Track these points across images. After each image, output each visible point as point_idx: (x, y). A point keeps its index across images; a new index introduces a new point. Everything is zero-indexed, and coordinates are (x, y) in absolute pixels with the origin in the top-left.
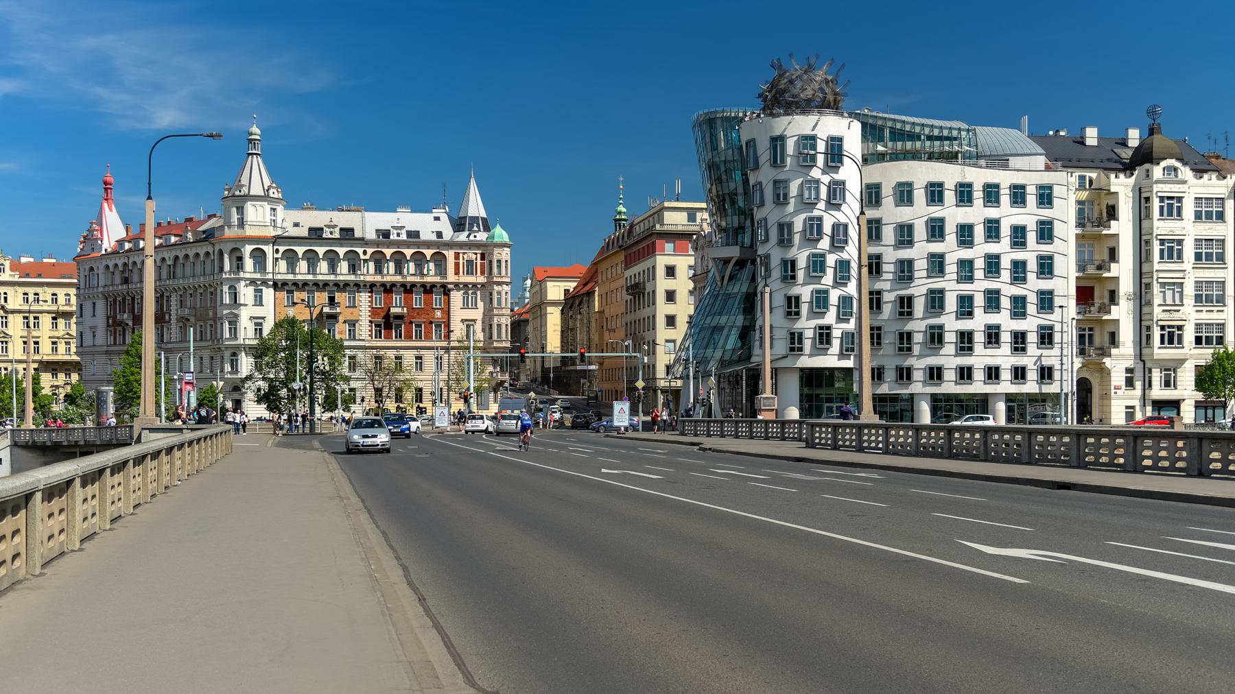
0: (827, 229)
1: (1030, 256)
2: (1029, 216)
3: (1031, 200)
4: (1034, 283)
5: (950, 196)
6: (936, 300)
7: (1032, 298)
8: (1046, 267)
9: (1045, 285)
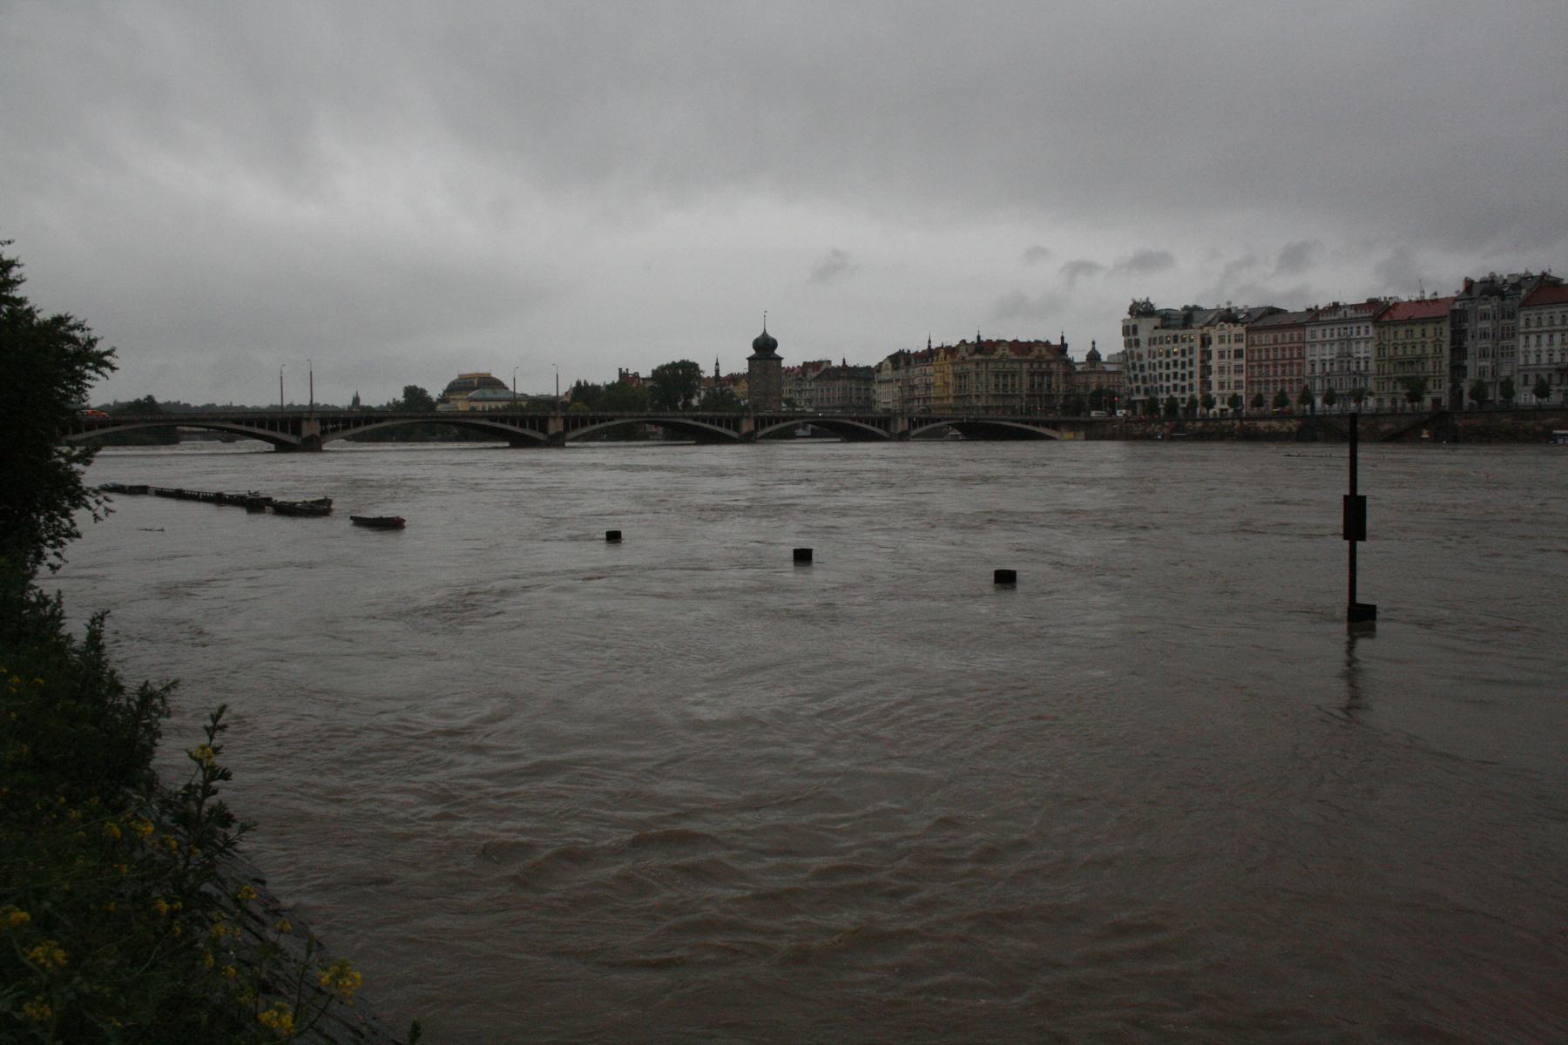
0: (1135, 355)
1: (1186, 360)
2: (1185, 346)
4: (1188, 369)
6: (1161, 375)
7: (1187, 374)
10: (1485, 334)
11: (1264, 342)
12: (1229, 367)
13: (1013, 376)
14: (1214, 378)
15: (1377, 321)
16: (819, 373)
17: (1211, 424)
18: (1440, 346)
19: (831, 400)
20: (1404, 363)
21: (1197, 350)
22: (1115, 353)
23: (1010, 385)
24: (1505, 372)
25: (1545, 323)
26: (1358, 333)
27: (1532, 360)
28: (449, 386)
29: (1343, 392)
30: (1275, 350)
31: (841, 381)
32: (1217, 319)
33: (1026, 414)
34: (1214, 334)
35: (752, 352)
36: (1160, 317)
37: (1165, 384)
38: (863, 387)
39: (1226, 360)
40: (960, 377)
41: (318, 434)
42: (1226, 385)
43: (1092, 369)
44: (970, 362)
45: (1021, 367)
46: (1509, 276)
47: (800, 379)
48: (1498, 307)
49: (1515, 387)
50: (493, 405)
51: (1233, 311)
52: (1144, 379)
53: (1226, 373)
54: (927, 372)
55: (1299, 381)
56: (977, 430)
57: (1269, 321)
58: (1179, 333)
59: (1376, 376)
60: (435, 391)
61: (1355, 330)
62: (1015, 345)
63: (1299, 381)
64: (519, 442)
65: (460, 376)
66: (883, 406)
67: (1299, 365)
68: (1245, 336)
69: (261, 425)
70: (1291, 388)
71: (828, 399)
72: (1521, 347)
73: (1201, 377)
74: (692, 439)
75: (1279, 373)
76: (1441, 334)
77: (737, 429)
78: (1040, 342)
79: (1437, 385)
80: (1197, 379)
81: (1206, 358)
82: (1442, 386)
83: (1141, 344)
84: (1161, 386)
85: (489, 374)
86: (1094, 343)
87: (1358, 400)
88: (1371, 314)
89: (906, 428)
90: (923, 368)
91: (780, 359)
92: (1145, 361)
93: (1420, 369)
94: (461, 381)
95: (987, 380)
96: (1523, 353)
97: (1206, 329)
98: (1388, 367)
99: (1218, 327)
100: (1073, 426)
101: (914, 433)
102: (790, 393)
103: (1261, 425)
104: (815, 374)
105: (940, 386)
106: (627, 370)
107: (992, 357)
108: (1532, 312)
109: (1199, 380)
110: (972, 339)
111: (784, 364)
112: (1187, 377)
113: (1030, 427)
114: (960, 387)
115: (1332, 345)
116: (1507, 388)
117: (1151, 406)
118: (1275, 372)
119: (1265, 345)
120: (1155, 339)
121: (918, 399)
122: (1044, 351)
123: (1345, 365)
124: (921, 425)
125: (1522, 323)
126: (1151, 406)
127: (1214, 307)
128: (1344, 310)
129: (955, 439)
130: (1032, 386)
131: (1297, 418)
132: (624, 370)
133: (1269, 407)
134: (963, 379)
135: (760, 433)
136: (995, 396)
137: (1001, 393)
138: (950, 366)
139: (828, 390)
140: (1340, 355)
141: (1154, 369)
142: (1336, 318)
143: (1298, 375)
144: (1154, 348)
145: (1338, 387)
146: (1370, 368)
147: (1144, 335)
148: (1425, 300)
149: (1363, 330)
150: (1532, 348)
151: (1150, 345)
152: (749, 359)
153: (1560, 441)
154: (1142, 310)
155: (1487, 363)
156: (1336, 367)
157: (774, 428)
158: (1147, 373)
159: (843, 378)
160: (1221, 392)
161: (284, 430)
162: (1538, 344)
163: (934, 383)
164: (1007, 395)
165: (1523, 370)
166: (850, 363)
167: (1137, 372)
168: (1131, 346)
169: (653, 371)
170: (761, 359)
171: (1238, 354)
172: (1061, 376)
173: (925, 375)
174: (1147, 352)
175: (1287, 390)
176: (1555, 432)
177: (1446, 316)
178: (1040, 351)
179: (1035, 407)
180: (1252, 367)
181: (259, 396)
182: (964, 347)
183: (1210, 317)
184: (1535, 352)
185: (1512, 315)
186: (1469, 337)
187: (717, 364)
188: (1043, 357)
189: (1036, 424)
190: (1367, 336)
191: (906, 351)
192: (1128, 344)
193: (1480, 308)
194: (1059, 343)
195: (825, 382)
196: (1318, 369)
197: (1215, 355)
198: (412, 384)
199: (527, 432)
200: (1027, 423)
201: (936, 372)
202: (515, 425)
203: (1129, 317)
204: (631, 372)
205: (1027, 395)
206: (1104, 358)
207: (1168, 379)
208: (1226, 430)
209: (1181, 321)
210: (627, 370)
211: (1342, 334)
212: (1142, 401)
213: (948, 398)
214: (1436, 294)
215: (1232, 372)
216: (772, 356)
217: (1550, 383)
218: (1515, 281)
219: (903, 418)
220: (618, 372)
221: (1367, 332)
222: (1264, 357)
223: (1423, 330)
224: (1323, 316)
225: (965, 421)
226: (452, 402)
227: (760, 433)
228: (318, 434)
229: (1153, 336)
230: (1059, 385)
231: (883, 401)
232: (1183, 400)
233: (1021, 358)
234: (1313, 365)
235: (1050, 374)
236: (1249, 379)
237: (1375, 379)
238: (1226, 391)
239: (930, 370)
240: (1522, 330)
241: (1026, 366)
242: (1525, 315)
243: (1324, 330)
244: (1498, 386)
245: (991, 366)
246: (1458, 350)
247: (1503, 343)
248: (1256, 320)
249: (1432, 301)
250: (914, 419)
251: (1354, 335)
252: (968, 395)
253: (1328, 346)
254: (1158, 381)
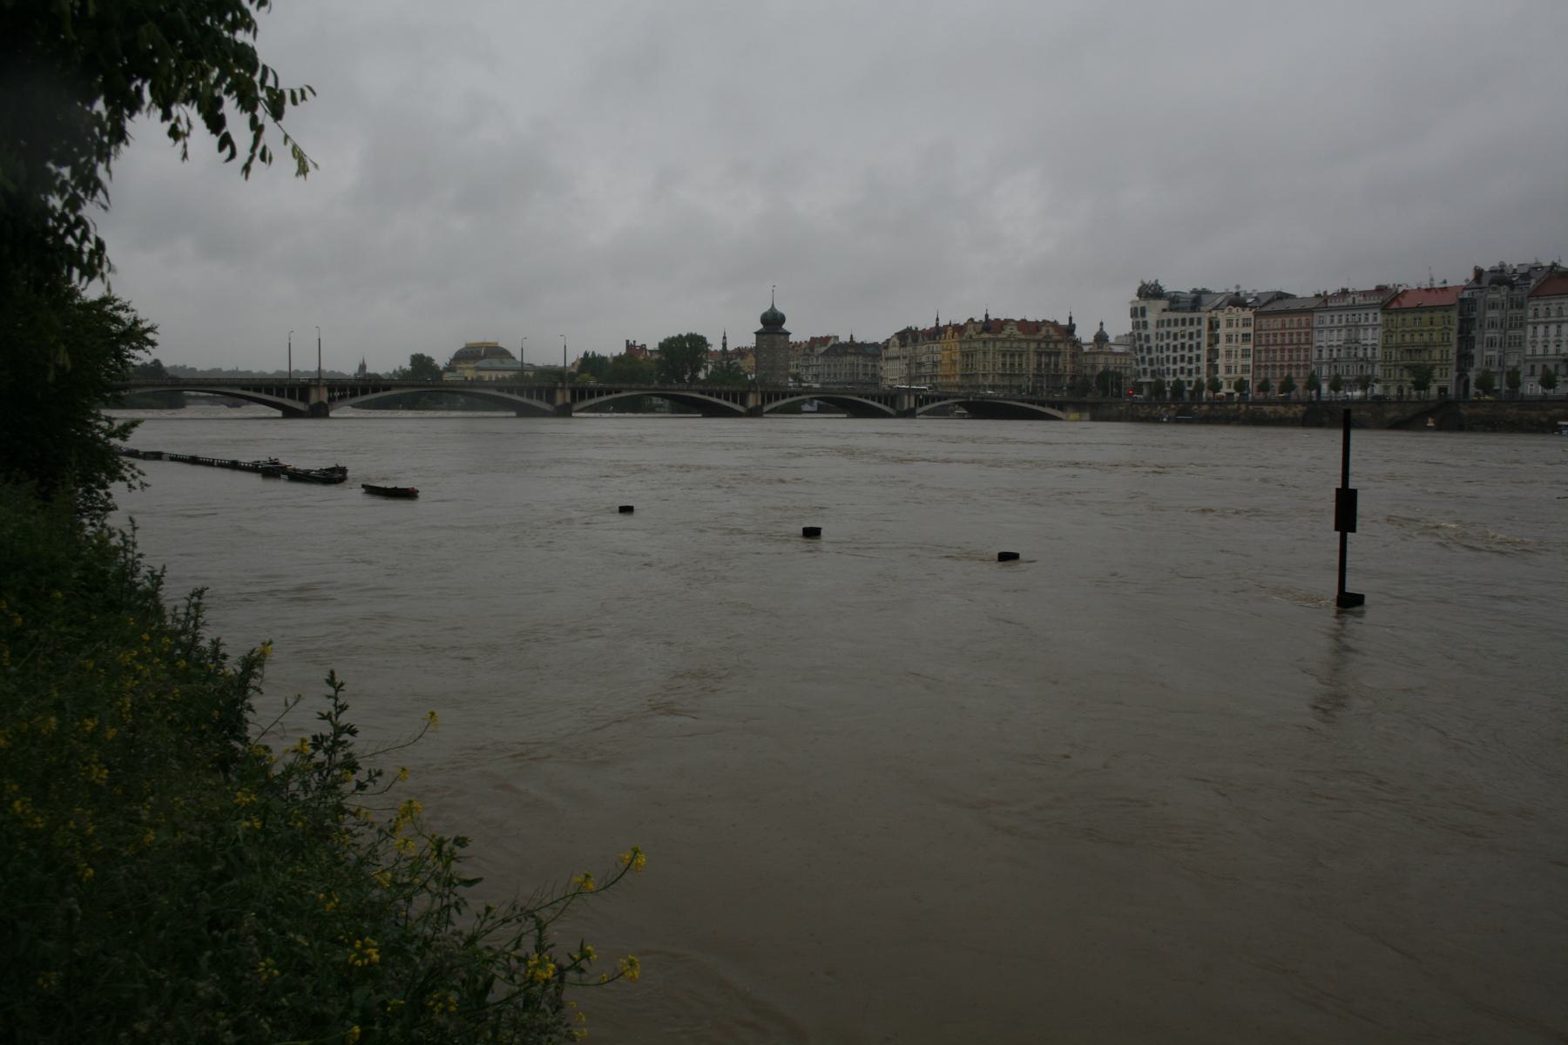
0: (1143, 336)
1: (1194, 343)
2: (1193, 329)
3: (1195, 323)
4: (1195, 352)
5: (1172, 323)
6: (1168, 357)
7: (1194, 357)
8: (1199, 345)
9: (1199, 352)
10: (1493, 323)
11: (1271, 327)
12: (1236, 351)
13: (1020, 356)
14: (1221, 362)
15: (1385, 308)
16: (825, 348)
17: (1217, 407)
18: (1448, 334)
19: (838, 376)
20: (1411, 350)
21: (1205, 333)
22: (1123, 334)
23: (1017, 364)
24: (1512, 362)
25: (1553, 314)
26: (1367, 319)
27: (1540, 350)
28: (456, 354)
29: (1350, 378)
30: (1283, 335)
31: (848, 358)
32: (1226, 303)
33: (1031, 394)
34: (1222, 317)
35: (760, 327)
36: (1168, 299)
37: (1172, 367)
39: (1233, 344)
40: (967, 355)
41: (326, 401)
42: (1233, 369)
43: (1100, 350)
44: (977, 340)
45: (1028, 347)
46: (1519, 265)
47: (807, 354)
48: (1507, 296)
49: (1521, 376)
50: (500, 374)
51: (1242, 295)
52: (1151, 360)
53: (1233, 356)
54: (935, 349)
55: (1306, 367)
56: (981, 409)
57: (1277, 306)
58: (1188, 316)
59: (1382, 363)
60: (441, 360)
61: (1363, 317)
62: (1023, 325)
63: (1306, 367)
64: (525, 412)
65: (466, 345)
66: (890, 383)
67: (1306, 350)
68: (1253, 319)
69: (269, 392)
70: (1298, 373)
71: (835, 375)
72: (1529, 338)
73: (1209, 360)
74: (699, 413)
75: (1286, 358)
76: (1449, 322)
77: (743, 403)
78: (1048, 322)
79: (1444, 374)
80: (1204, 363)
81: (1213, 342)
82: (1449, 374)
83: (1149, 326)
84: (1168, 369)
85: (497, 343)
86: (1102, 324)
87: (1364, 388)
88: (1380, 301)
89: (912, 405)
90: (931, 345)
91: (788, 334)
92: (1153, 343)
93: (1427, 357)
94: (468, 350)
95: (994, 358)
96: (1531, 342)
97: (1214, 312)
98: (1396, 355)
99: (1226, 311)
100: (1079, 407)
101: (919, 410)
102: (797, 367)
103: (1267, 409)
104: (823, 349)
105: (946, 364)
106: (634, 342)
107: (1000, 336)
108: (1542, 303)
109: (1206, 363)
110: (979, 317)
111: (792, 339)
112: (1194, 361)
113: (1035, 407)
114: (967, 365)
115: (1339, 331)
116: (1514, 379)
117: (1158, 388)
118: (1282, 357)
119: (1274, 329)
120: (1163, 321)
121: (925, 377)
122: (1052, 331)
123: (1353, 352)
124: (927, 403)
125: (1531, 313)
126: (1158, 388)
127: (1223, 291)
128: (1352, 296)
129: (961, 416)
130: (1039, 365)
131: (1304, 404)
132: (631, 342)
133: (1275, 393)
134: (970, 357)
135: (766, 408)
137: (1008, 372)
138: (957, 343)
139: (835, 365)
140: (1348, 341)
141: (1162, 352)
142: (1345, 304)
143: (1305, 361)
144: (1162, 330)
145: (1345, 373)
146: (1377, 355)
147: (1152, 317)
148: (1434, 289)
149: (1371, 317)
150: (1540, 338)
151: (1157, 327)
152: (756, 333)
153: (1565, 432)
154: (1150, 292)
155: (1494, 353)
156: (1343, 354)
157: (782, 402)
158: (1154, 355)
159: (851, 354)
160: (1229, 376)
161: (291, 396)
162: (1546, 334)
163: (940, 361)
164: (1015, 375)
165: (1531, 361)
166: (858, 340)
167: (1145, 353)
168: (1139, 328)
169: (660, 344)
170: (769, 333)
171: (1246, 337)
172: (1068, 358)
173: (932, 352)
174: (1155, 335)
175: (1294, 375)
176: (1560, 423)
177: (1453, 305)
178: (1048, 331)
179: (1042, 387)
180: (1260, 352)
181: (267, 362)
182: (972, 326)
183: (1218, 301)
184: (1543, 342)
185: (1521, 306)
186: (1477, 324)
187: (725, 338)
188: (1050, 337)
189: (1042, 404)
190: (1375, 323)
191: (914, 328)
192: (1136, 326)
193: (1490, 296)
194: (1067, 323)
195: (832, 358)
196: (1325, 354)
197: (1223, 339)
198: (419, 353)
199: (535, 402)
200: (1033, 403)
201: (943, 350)
202: (521, 395)
203: (1137, 298)
204: (638, 344)
205: (1034, 375)
206: (1112, 339)
207: (1175, 361)
208: (1232, 414)
209: (1188, 305)
210: (634, 342)
211: (1350, 320)
212: (1150, 383)
213: (954, 376)
214: (1445, 282)
215: (1239, 357)
216: (780, 331)
217: (1557, 374)
218: (1525, 270)
219: (909, 396)
220: (625, 343)
221: (1375, 319)
222: (1271, 342)
223: (1432, 318)
224: (1331, 302)
225: (971, 399)
226: (458, 371)
227: (766, 408)
228: (326, 401)
229: (1161, 319)
230: (1066, 365)
231: (890, 377)
232: (1190, 383)
233: (1031, 337)
234: (1320, 351)
235: (1058, 354)
236: (1257, 364)
237: (1382, 366)
238: (1233, 375)
239: (937, 347)
240: (1530, 320)
241: (1033, 346)
242: (1533, 305)
243: (1332, 316)
244: (1504, 377)
245: (998, 345)
246: (1466, 338)
247: (1511, 332)
248: (1266, 304)
249: (1440, 289)
250: (921, 397)
251: (1362, 322)
252: (977, 374)
253: (1335, 332)
254: (1165, 363)
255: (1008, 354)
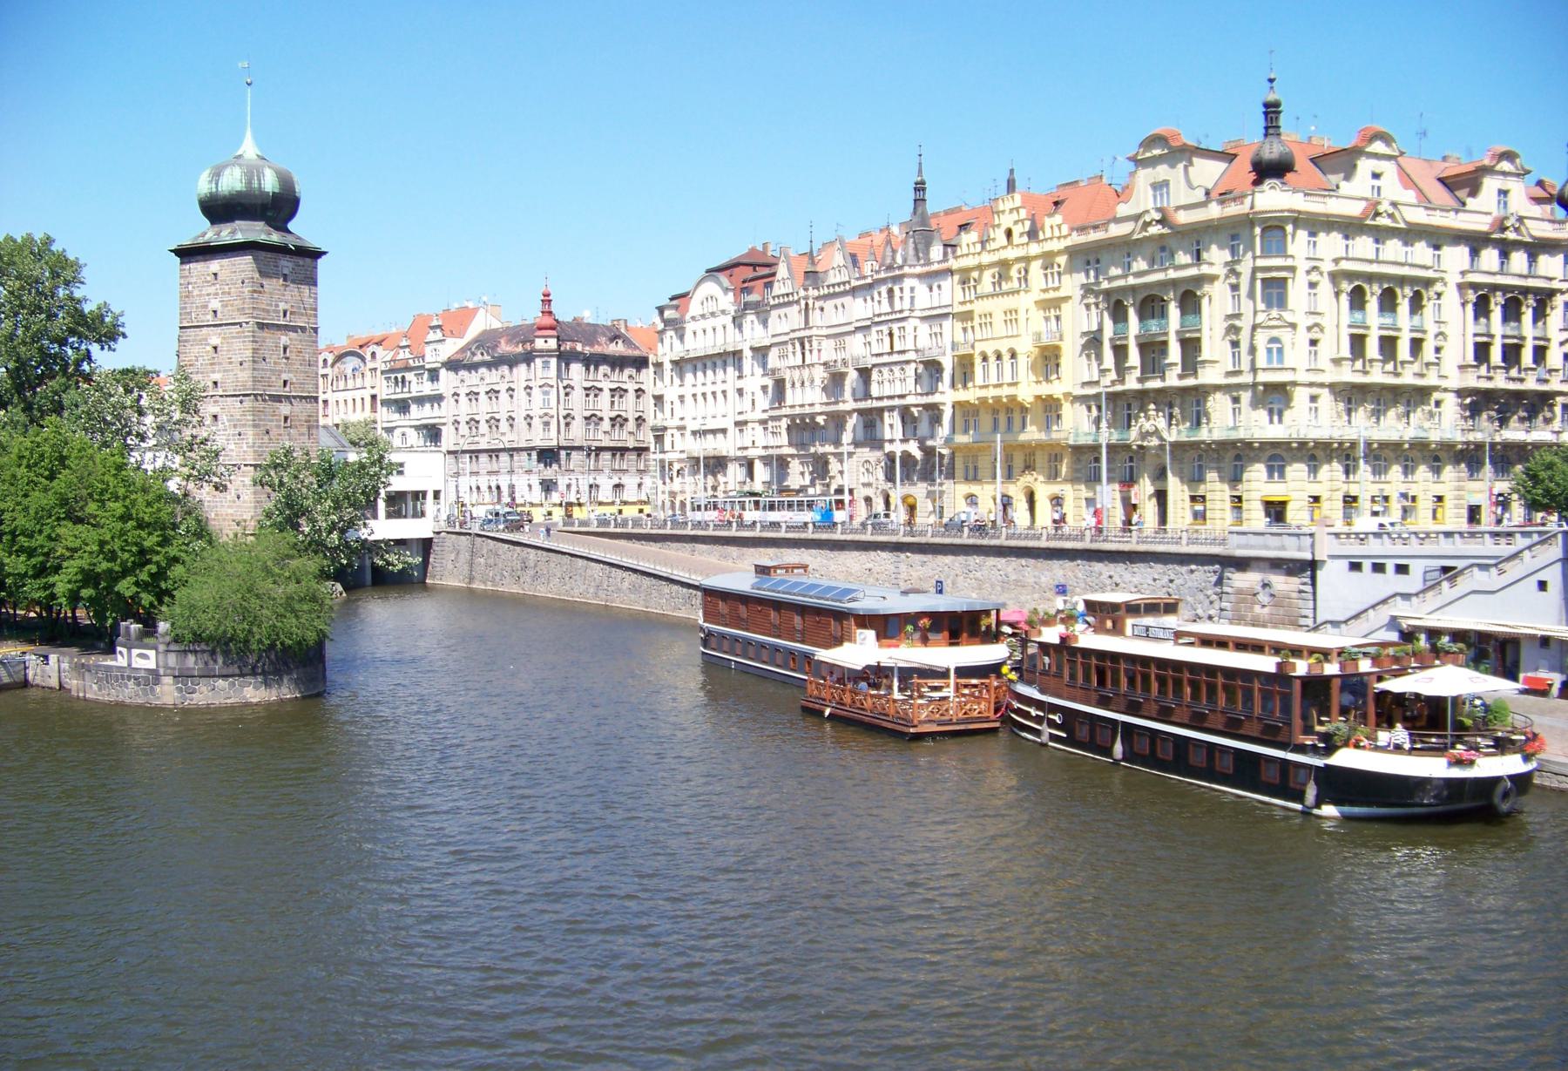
38: (606, 385)
104: (451, 348)
136: (1351, 395)
245: (1331, 245)
255: (1377, 289)
